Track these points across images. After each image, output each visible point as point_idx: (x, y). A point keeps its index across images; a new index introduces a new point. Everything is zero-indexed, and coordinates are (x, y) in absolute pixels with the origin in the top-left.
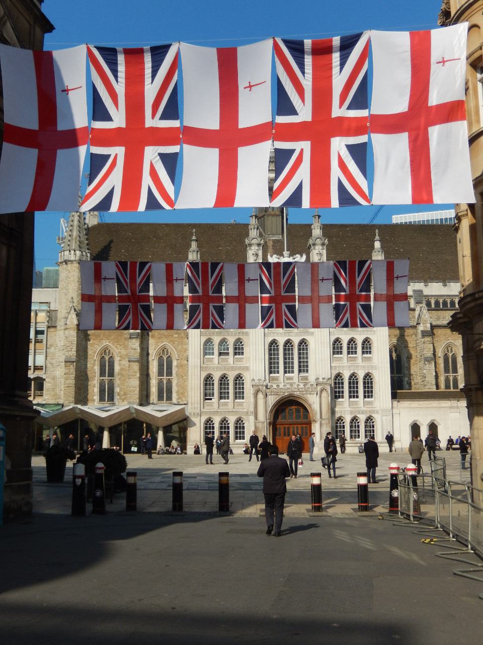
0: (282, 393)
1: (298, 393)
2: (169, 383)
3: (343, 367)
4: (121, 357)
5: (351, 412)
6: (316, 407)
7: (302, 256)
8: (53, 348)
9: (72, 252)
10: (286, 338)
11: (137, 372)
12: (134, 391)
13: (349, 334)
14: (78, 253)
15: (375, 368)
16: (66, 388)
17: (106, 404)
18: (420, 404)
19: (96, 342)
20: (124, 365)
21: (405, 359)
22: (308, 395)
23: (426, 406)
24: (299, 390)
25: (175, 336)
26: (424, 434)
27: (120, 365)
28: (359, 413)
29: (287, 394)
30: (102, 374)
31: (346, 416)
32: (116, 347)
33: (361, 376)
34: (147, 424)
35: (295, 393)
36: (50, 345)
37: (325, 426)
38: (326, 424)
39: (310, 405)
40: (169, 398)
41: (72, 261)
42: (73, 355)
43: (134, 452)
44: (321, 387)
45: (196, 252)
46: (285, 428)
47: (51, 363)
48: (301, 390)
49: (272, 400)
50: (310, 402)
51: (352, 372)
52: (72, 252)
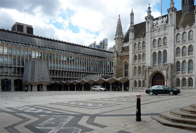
6: (165, 75)
7: (165, 18)
22: (163, 71)
46: (157, 83)
49: (151, 73)
51: (183, 60)
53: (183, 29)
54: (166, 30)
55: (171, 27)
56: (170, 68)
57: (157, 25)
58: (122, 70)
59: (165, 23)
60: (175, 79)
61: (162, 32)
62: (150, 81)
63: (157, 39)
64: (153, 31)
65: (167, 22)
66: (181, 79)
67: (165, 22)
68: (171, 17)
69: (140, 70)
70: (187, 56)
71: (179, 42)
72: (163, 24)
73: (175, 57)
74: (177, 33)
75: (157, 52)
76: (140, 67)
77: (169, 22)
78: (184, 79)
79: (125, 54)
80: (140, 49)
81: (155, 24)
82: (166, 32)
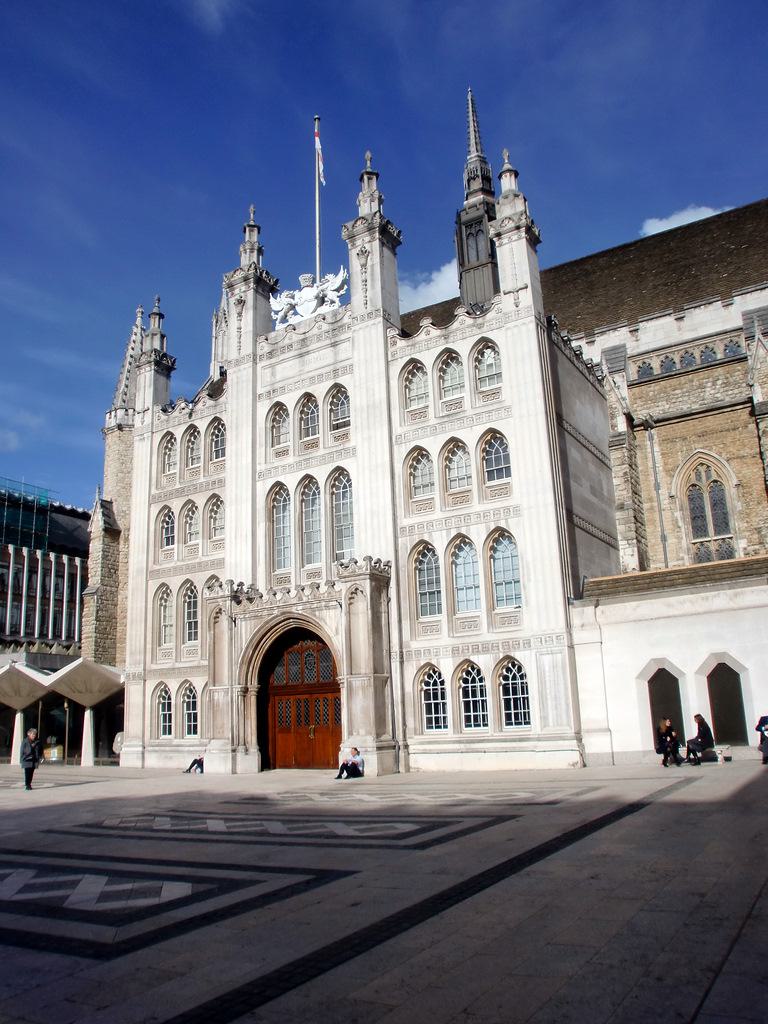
0: (265, 613)
1: (301, 608)
3: (430, 523)
5: (455, 651)
6: (337, 643)
7: (336, 274)
10: (302, 474)
13: (444, 432)
15: (517, 510)
18: (669, 605)
21: (734, 491)
22: (325, 613)
23: (688, 608)
24: (300, 599)
26: (695, 702)
28: (476, 649)
29: (276, 612)
31: (442, 661)
33: (478, 535)
35: (294, 609)
37: (360, 692)
38: (363, 688)
44: (349, 584)
45: (159, 336)
48: (305, 599)
49: (247, 631)
50: (326, 628)
51: (454, 533)
52: (113, 413)
53: (435, 332)
54: (342, 347)
55: (372, 322)
56: (366, 585)
57: (293, 320)
59: (338, 303)
60: (411, 670)
61: (321, 358)
62: (245, 691)
63: (290, 400)
64: (271, 354)
65: (345, 300)
66: (447, 668)
67: (337, 300)
68: (364, 266)
69: (190, 609)
70: (476, 506)
71: (422, 413)
72: (325, 309)
73: (400, 512)
74: (407, 358)
76: (189, 588)
77: (357, 298)
78: (470, 673)
80: (196, 472)
81: (281, 314)
82: (342, 356)
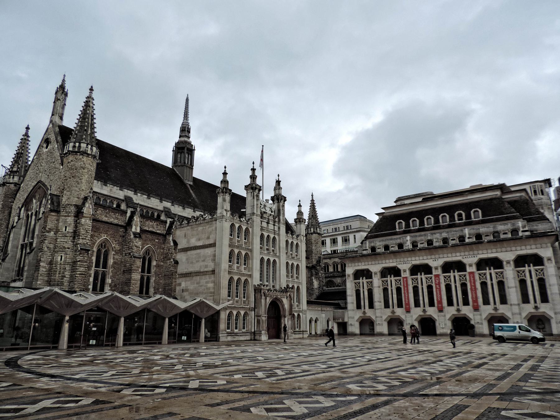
2: (148, 279)
4: (115, 251)
8: (52, 233)
9: (89, 146)
11: (139, 267)
12: (136, 284)
14: (94, 149)
16: (78, 276)
17: (96, 294)
19: (96, 234)
20: (117, 259)
25: (157, 241)
27: (114, 258)
30: (97, 265)
32: (112, 242)
34: (195, 315)
36: (50, 229)
39: (283, 305)
40: (147, 292)
41: (88, 154)
42: (87, 243)
43: (184, 342)
47: (48, 248)
58: (89, 268)
72: (270, 213)
75: (266, 258)
79: (105, 219)
